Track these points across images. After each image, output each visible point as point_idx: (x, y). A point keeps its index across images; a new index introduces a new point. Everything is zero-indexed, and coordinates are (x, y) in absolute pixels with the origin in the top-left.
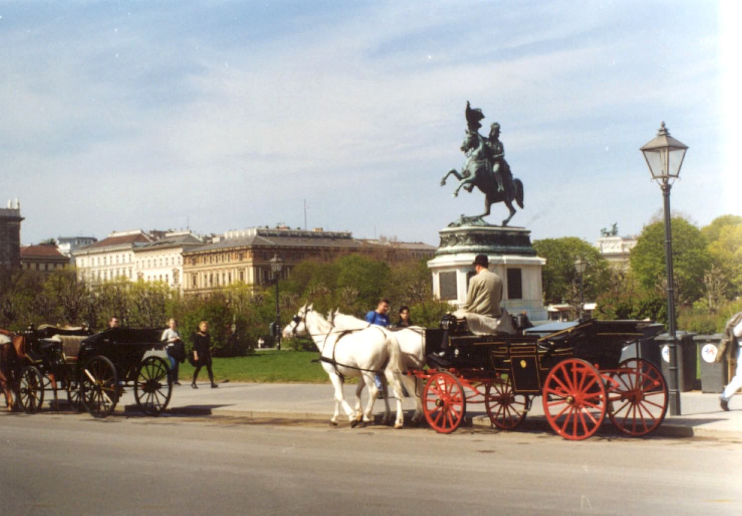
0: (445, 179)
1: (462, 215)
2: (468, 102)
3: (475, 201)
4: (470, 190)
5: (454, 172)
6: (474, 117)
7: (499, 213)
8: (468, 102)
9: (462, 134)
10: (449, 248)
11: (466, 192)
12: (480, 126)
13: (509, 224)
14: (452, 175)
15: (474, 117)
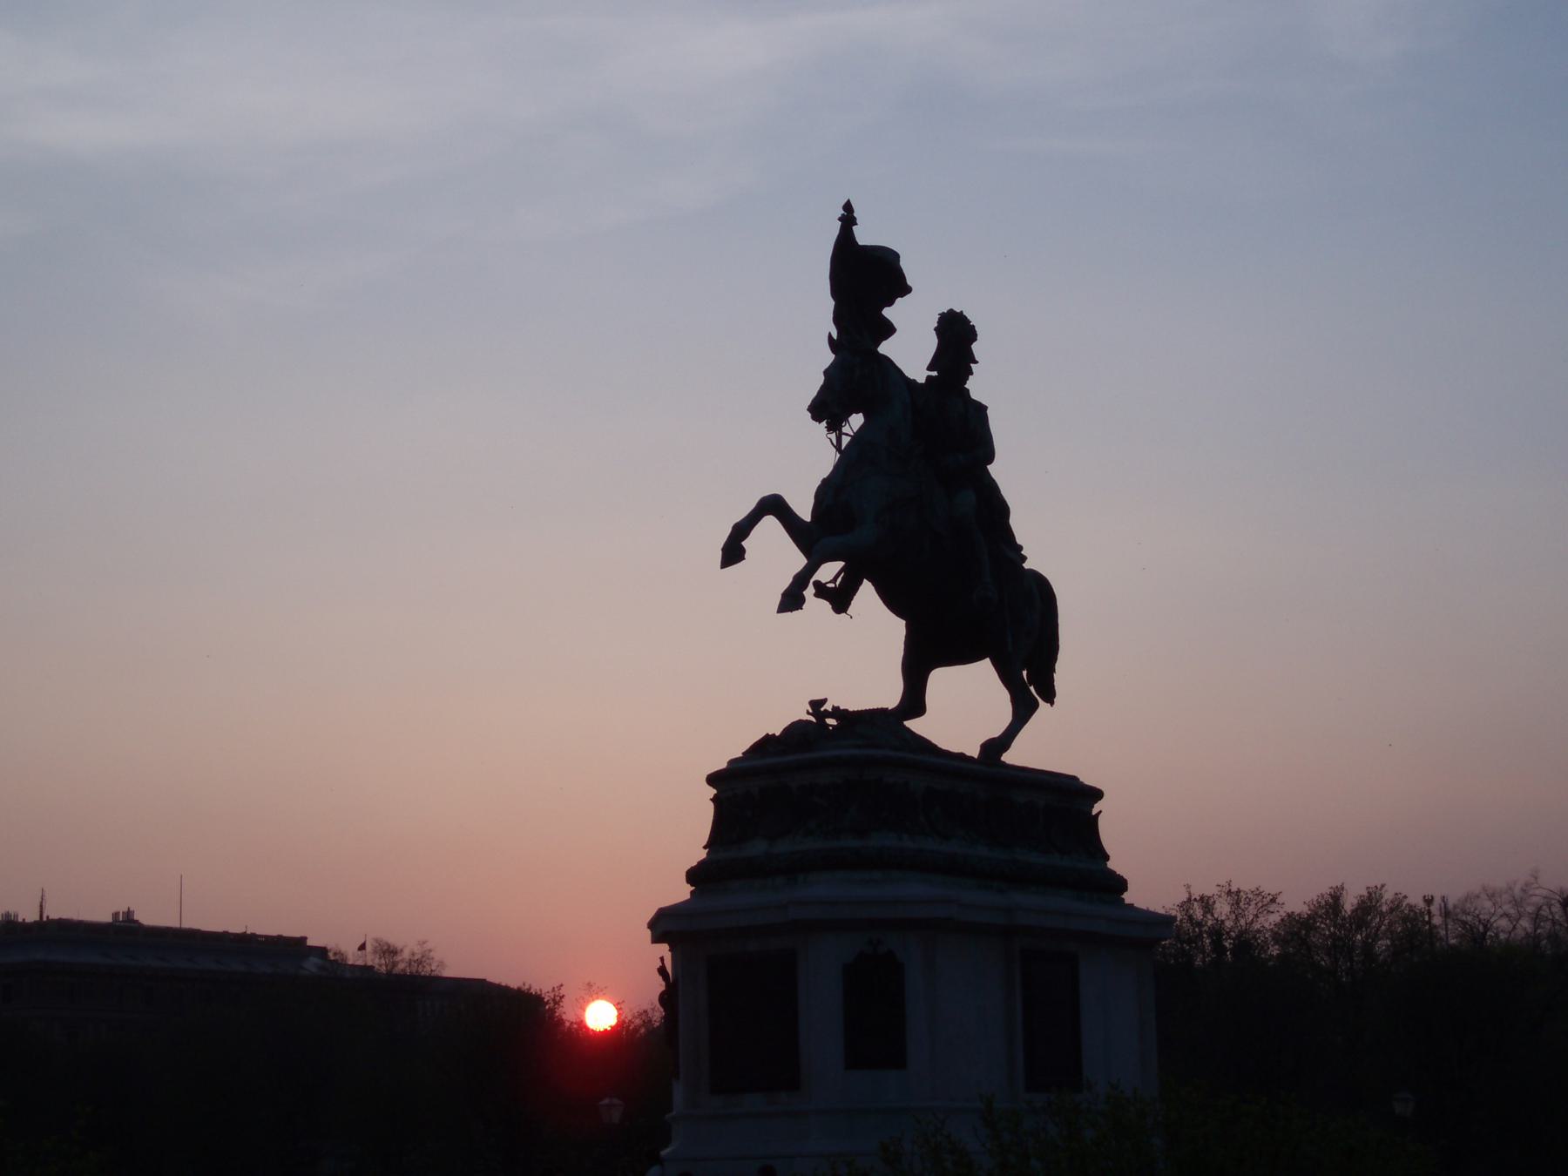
0: (742, 530)
1: (816, 705)
2: (848, 207)
3: (855, 654)
4: (840, 599)
5: (773, 506)
6: (865, 280)
7: (964, 707)
8: (848, 207)
9: (811, 360)
10: (757, 848)
11: (825, 605)
12: (888, 330)
13: (1010, 757)
14: (770, 524)
15: (865, 280)
